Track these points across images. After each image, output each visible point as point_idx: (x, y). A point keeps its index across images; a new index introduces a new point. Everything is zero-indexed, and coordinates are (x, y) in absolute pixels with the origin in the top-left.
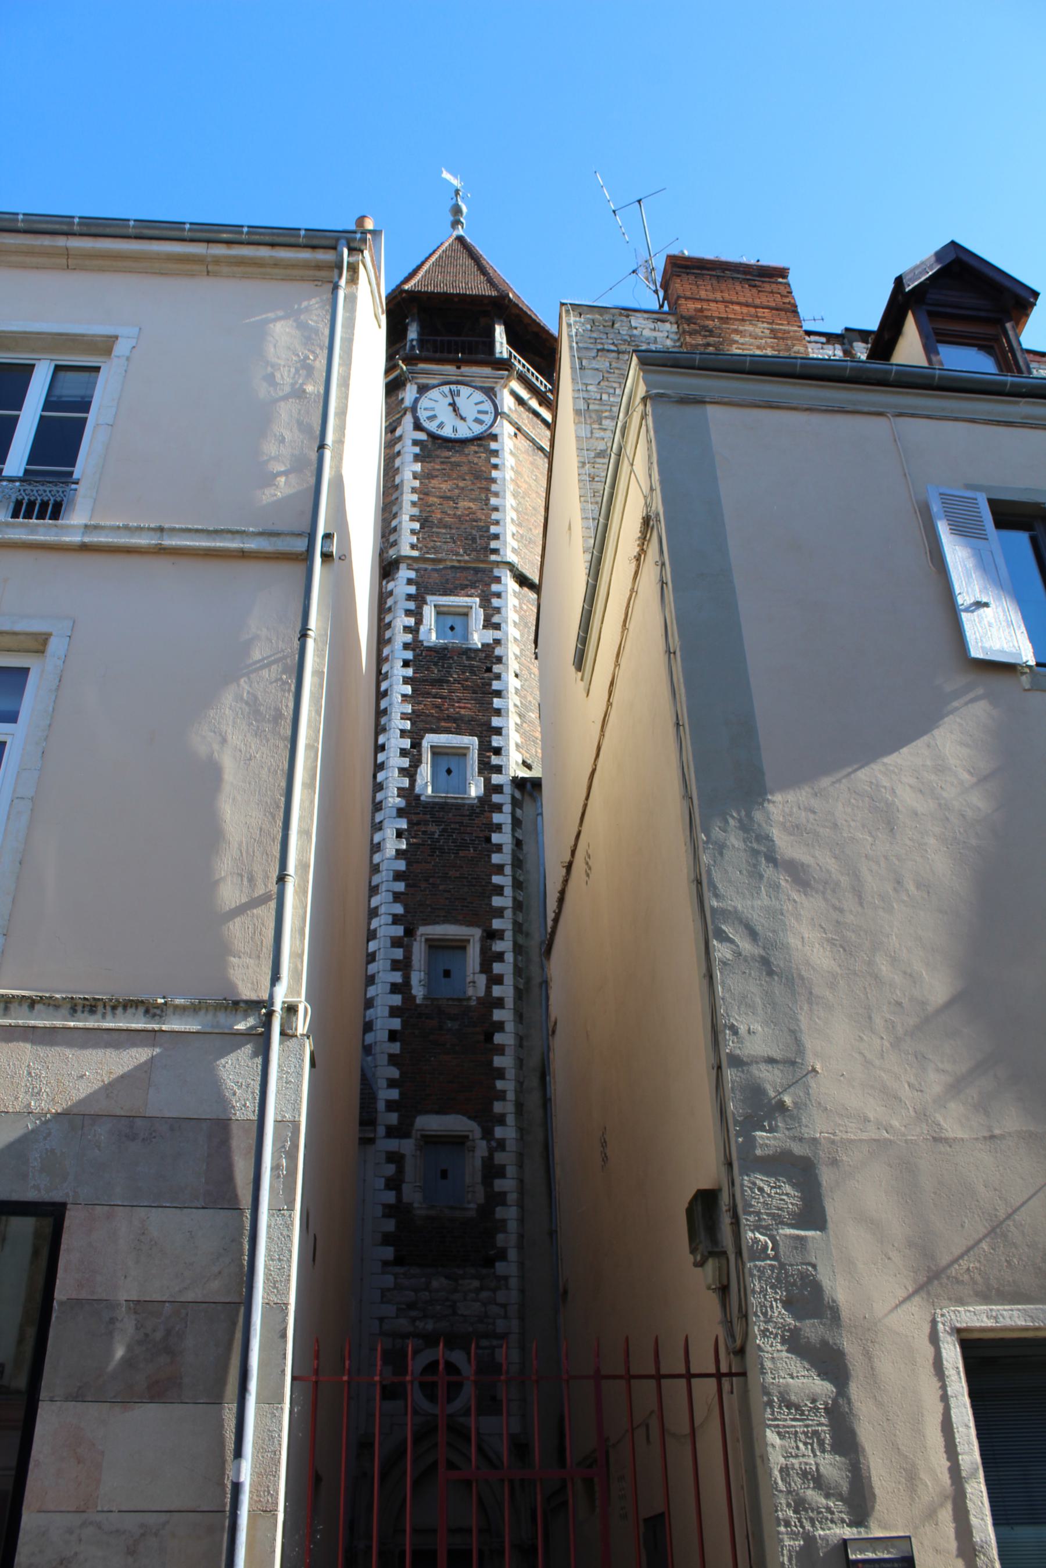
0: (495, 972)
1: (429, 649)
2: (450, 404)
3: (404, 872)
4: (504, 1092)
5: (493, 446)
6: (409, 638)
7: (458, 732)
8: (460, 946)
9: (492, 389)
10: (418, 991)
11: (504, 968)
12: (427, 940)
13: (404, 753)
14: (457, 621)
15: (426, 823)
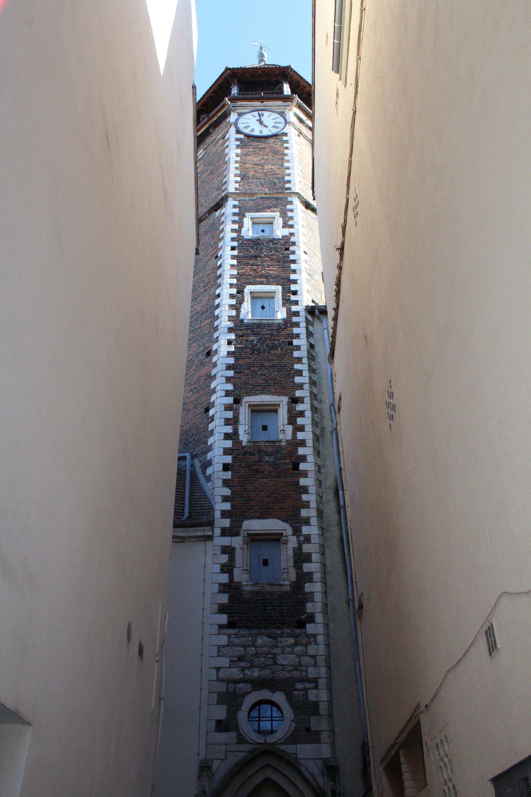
0: (299, 423)
1: (248, 240)
2: (258, 120)
3: (233, 364)
4: (308, 502)
5: (285, 138)
6: (235, 235)
7: (268, 283)
8: (273, 410)
9: (283, 112)
10: (244, 438)
11: (305, 421)
13: (232, 296)
14: (266, 228)
15: (248, 335)
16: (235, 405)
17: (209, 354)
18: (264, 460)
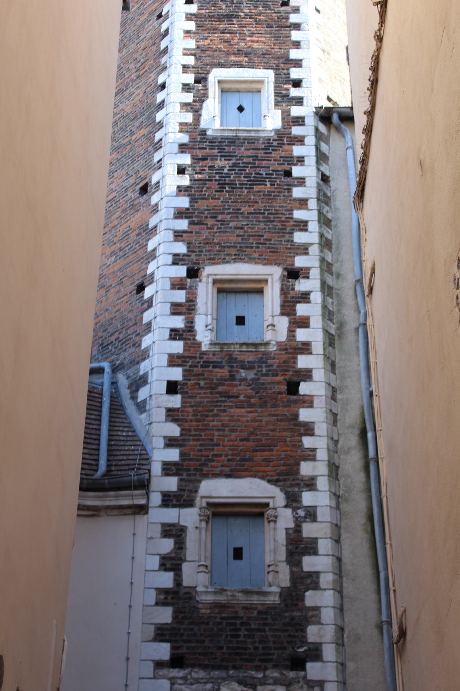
3: (187, 209)
7: (251, 65)
8: (256, 289)
10: (204, 337)
11: (311, 310)
12: (215, 282)
13: (186, 88)
15: (214, 158)
16: (189, 280)
17: (144, 190)
18: (238, 377)
